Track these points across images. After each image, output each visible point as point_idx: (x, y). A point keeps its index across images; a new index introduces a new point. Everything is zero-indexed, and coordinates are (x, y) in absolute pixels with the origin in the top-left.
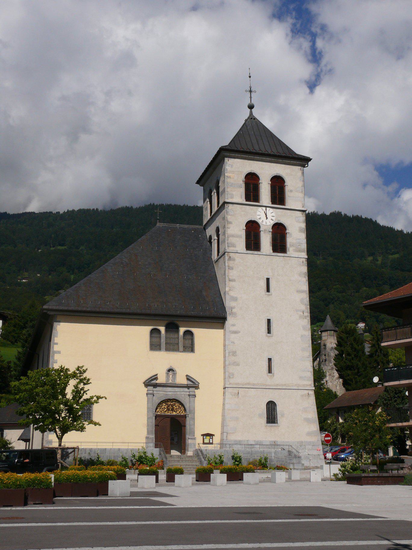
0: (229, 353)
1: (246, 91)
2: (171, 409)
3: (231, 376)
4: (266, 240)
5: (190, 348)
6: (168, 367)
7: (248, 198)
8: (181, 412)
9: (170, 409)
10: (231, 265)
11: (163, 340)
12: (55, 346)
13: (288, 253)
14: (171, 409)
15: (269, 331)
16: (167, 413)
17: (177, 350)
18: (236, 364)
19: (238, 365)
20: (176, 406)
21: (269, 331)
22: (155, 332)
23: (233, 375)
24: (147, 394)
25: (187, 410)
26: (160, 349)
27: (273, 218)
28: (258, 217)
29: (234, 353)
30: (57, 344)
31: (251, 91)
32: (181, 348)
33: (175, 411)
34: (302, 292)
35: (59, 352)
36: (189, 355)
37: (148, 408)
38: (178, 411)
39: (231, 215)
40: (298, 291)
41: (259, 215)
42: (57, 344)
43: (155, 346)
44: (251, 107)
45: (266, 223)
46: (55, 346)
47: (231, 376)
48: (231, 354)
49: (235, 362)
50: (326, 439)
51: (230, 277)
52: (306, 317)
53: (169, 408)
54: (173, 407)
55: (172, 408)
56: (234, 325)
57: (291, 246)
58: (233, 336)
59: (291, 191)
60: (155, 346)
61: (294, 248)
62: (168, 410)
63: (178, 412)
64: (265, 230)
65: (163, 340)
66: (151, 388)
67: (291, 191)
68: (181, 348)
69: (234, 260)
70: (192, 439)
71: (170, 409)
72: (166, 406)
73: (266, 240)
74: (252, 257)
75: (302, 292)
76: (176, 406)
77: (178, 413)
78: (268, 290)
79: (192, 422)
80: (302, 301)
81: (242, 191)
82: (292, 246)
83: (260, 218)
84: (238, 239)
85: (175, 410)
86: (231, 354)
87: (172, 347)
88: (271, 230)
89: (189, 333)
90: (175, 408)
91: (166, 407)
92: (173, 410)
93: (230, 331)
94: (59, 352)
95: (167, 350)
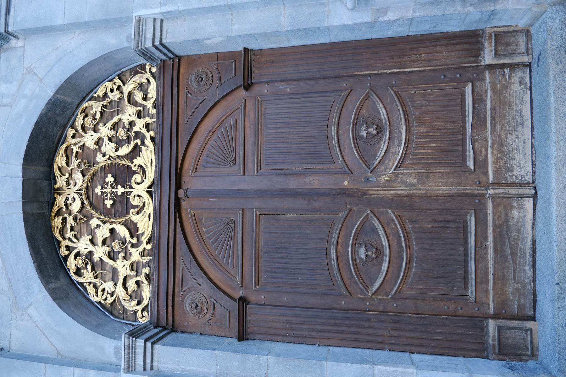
2: (117, 181)
8: (138, 96)
9: (120, 190)
14: (117, 181)
20: (99, 142)
33: (135, 152)
38: (131, 124)
53: (109, 203)
54: (105, 170)
55: (110, 179)
63: (139, 125)
71: (120, 190)
72: (94, 222)
76: (99, 142)
77: (147, 126)
85: (125, 150)
90: (108, 148)
91: (103, 232)
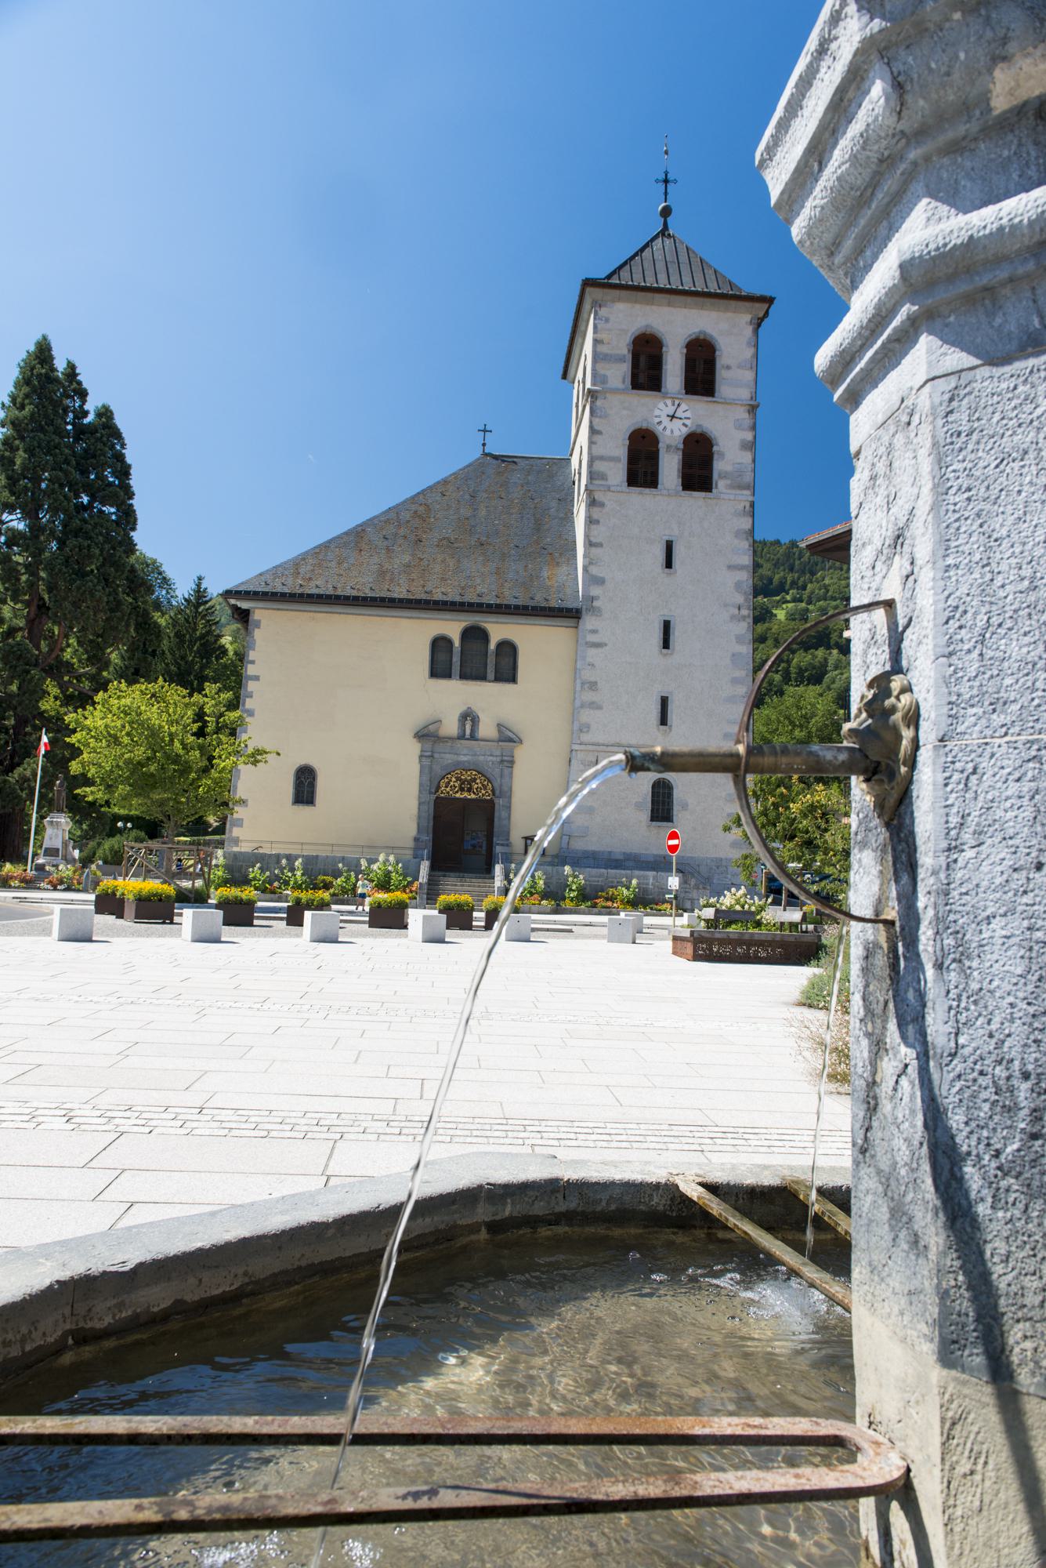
0: (583, 684)
1: (657, 181)
3: (584, 728)
4: (670, 467)
5: (507, 673)
6: (463, 708)
7: (636, 384)
10: (595, 516)
11: (456, 659)
12: (250, 666)
13: (714, 490)
15: (666, 644)
16: (458, 795)
17: (482, 677)
18: (594, 706)
19: (600, 708)
21: (666, 644)
22: (440, 644)
23: (588, 727)
24: (421, 756)
25: (497, 792)
26: (447, 675)
27: (688, 422)
28: (657, 420)
29: (593, 686)
30: (253, 662)
31: (666, 181)
32: (491, 674)
34: (741, 568)
35: (257, 678)
36: (507, 687)
37: (421, 785)
39: (600, 417)
40: (730, 567)
41: (659, 416)
42: (253, 662)
43: (439, 669)
44: (666, 212)
45: (672, 431)
46: (250, 666)
47: (584, 728)
48: (586, 686)
49: (593, 703)
50: (672, 842)
51: (592, 539)
52: (744, 618)
56: (594, 632)
57: (720, 477)
58: (592, 652)
59: (728, 368)
60: (439, 669)
61: (729, 482)
62: (462, 789)
64: (669, 447)
65: (456, 659)
66: (428, 746)
67: (728, 368)
68: (491, 674)
69: (602, 505)
70: (502, 845)
73: (670, 467)
74: (640, 497)
75: (741, 568)
78: (669, 564)
79: (504, 814)
80: (738, 586)
81: (625, 368)
82: (724, 475)
83: (660, 423)
84: (612, 464)
86: (586, 686)
87: (473, 672)
88: (681, 446)
89: (508, 650)
92: (469, 790)
93: (587, 643)
94: (257, 678)
95: (463, 676)
